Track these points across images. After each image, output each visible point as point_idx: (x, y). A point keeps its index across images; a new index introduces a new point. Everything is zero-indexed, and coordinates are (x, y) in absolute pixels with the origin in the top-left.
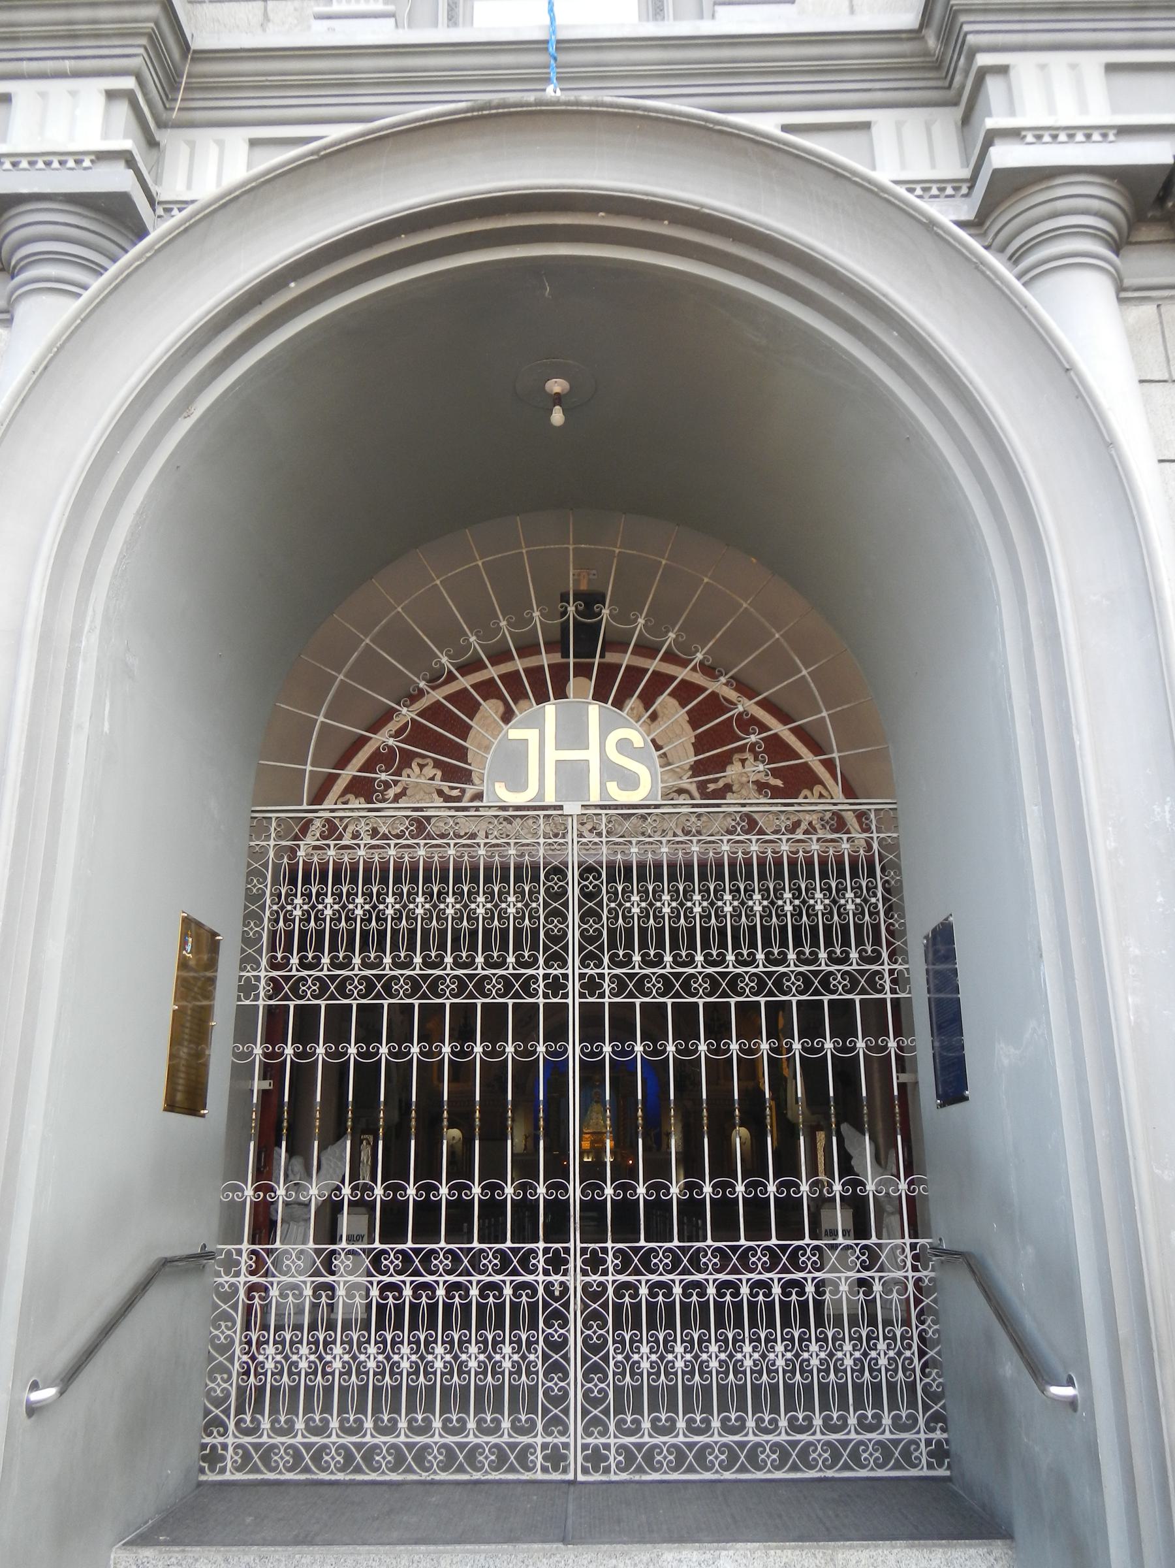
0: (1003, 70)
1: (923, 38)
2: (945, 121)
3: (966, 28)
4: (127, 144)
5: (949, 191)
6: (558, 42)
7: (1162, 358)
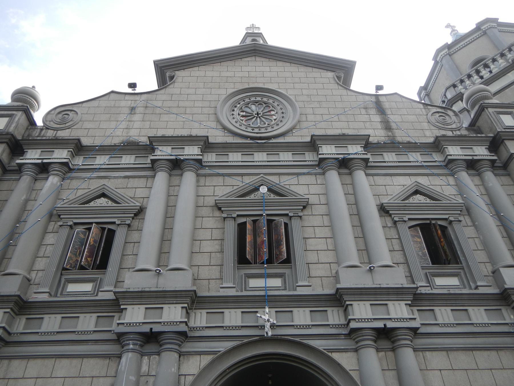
0: (351, 305)
1: (336, 296)
2: (341, 310)
3: (344, 297)
4: (186, 320)
5: (343, 326)
6: (267, 295)
7: (387, 365)
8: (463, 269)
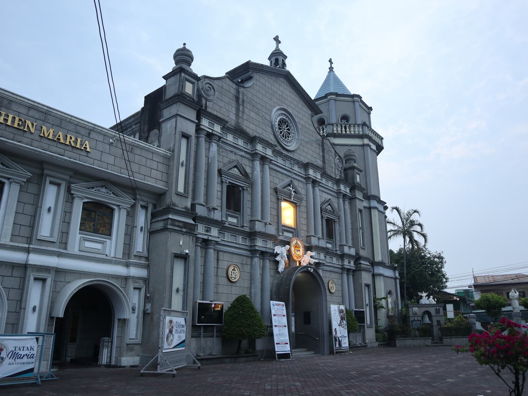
8: (240, 215)
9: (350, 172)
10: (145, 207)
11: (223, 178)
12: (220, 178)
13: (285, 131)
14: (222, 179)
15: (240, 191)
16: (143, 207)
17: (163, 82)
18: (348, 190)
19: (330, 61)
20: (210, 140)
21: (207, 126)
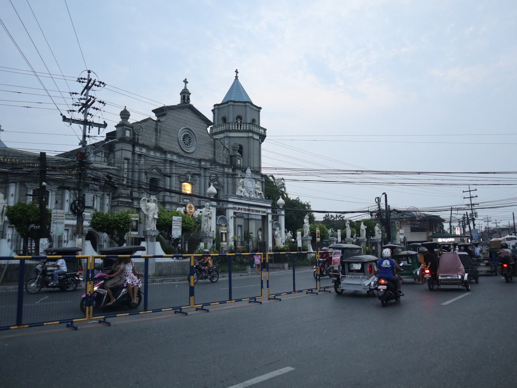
9: (234, 158)
10: (108, 195)
11: (148, 176)
12: (146, 176)
13: (188, 141)
14: (147, 176)
15: (158, 181)
16: (107, 194)
17: (115, 129)
18: (231, 171)
19: (237, 72)
20: (140, 157)
21: (138, 151)
